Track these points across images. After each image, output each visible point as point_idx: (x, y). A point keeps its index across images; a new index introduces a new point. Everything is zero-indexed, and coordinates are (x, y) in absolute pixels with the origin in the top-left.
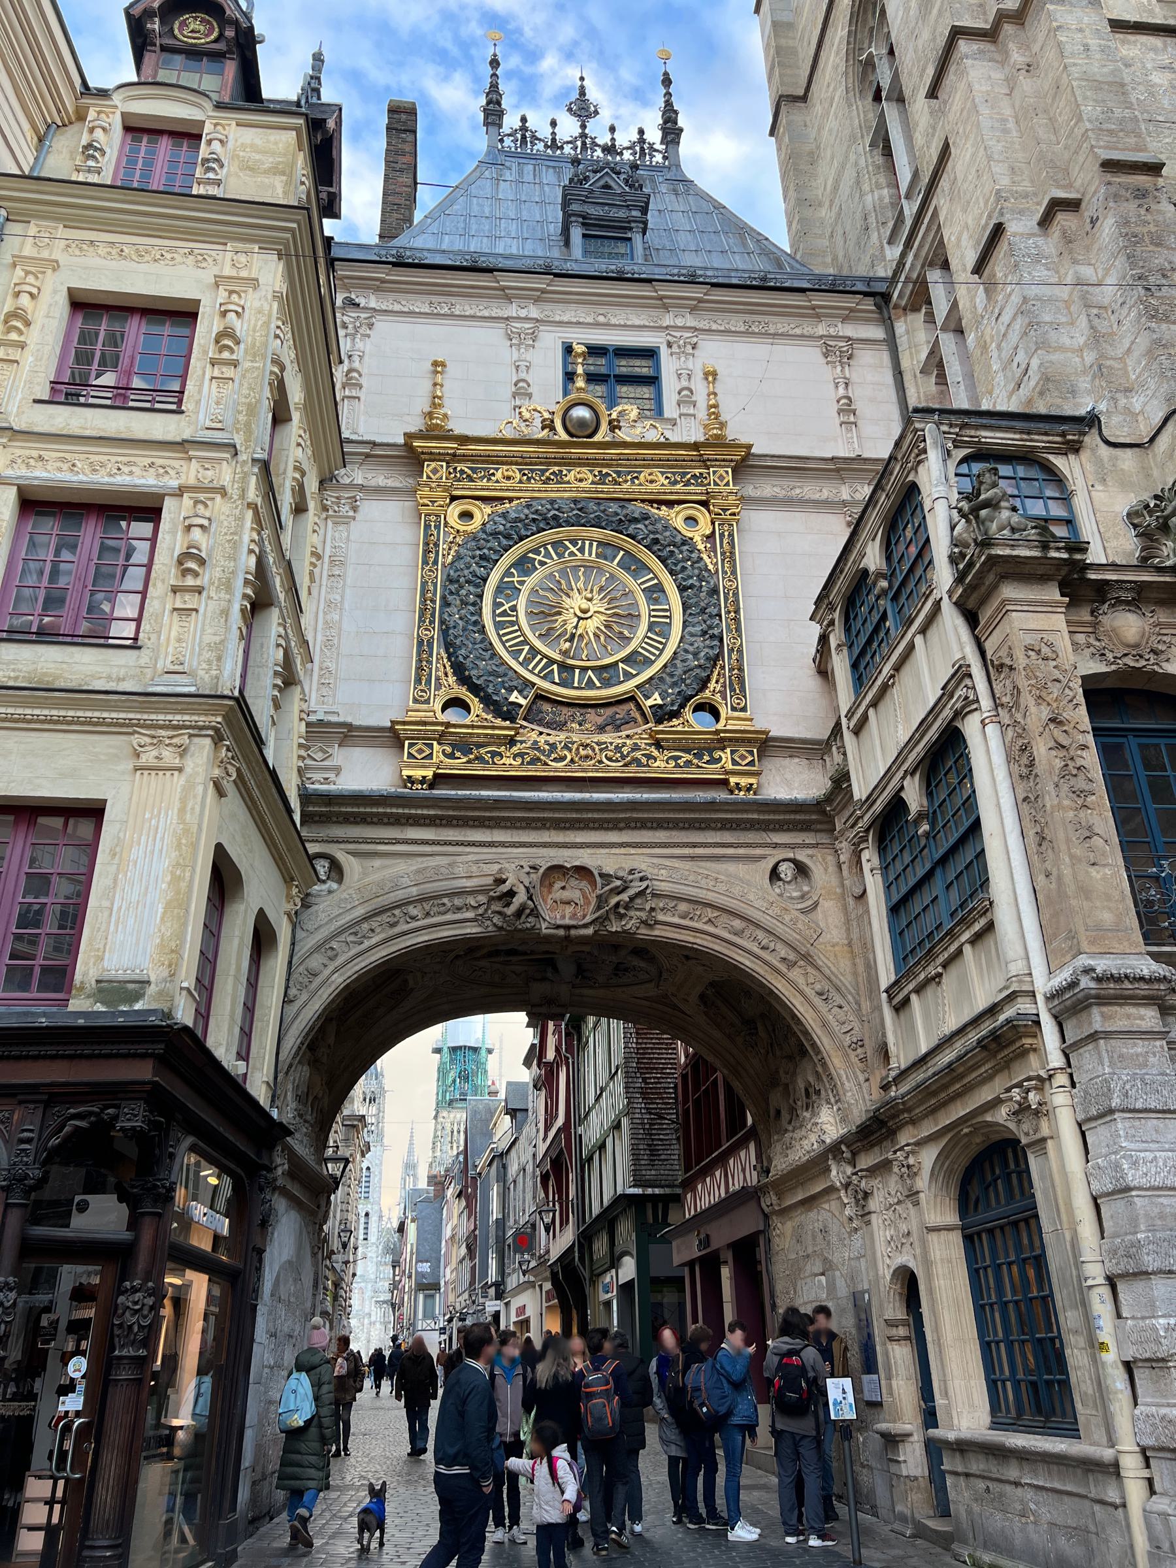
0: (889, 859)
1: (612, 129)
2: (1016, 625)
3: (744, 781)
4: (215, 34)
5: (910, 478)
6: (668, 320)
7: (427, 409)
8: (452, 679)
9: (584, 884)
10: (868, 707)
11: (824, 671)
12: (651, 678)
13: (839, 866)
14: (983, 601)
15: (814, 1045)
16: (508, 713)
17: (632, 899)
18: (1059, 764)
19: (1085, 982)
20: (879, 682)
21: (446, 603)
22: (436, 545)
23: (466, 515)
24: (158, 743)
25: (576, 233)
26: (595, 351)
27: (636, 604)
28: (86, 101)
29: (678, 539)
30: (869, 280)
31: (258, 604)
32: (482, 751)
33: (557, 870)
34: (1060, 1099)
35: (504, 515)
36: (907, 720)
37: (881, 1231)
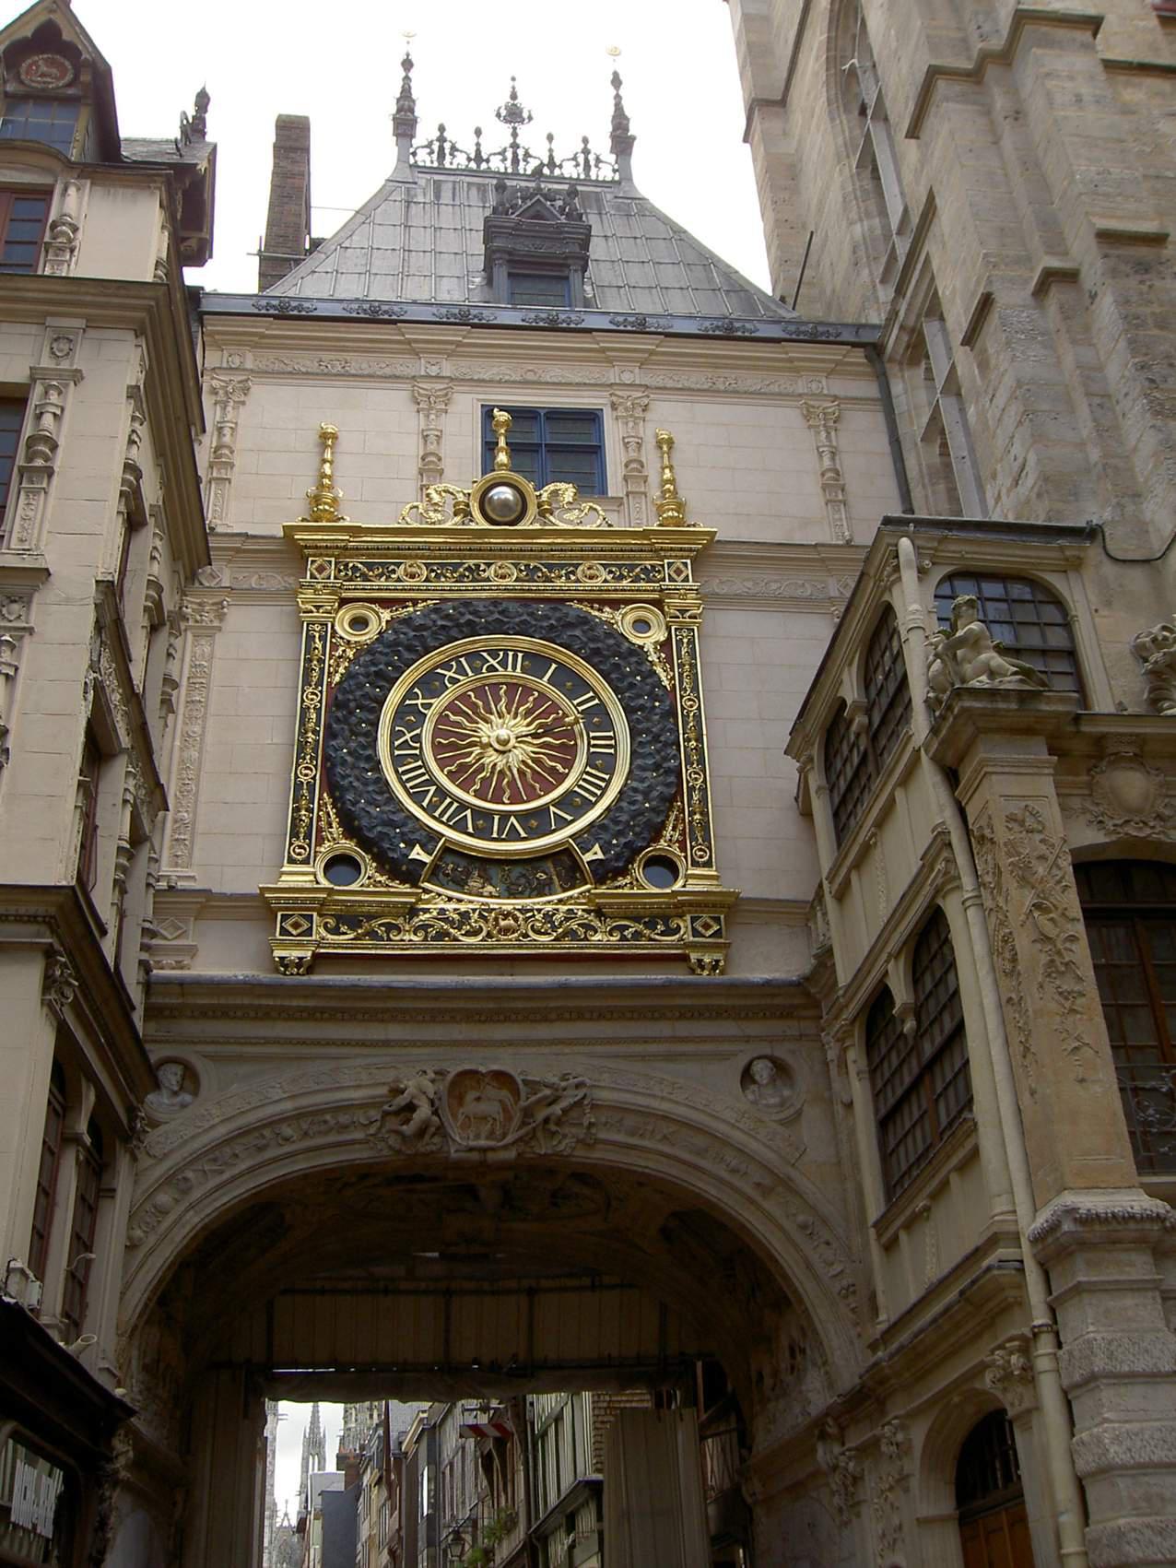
0: (877, 1060)
1: (550, 138)
4: (69, 77)
5: (886, 597)
6: (612, 375)
7: (312, 490)
8: (336, 830)
9: (505, 1094)
10: (849, 872)
11: (807, 814)
12: (592, 824)
14: (961, 759)
15: (796, 1291)
16: (410, 873)
17: (565, 1111)
18: (1044, 959)
19: (1067, 1226)
20: (860, 839)
21: (330, 734)
22: (321, 661)
23: (359, 623)
26: (519, 414)
30: (859, 327)
31: (97, 751)
32: (374, 923)
35: (407, 621)
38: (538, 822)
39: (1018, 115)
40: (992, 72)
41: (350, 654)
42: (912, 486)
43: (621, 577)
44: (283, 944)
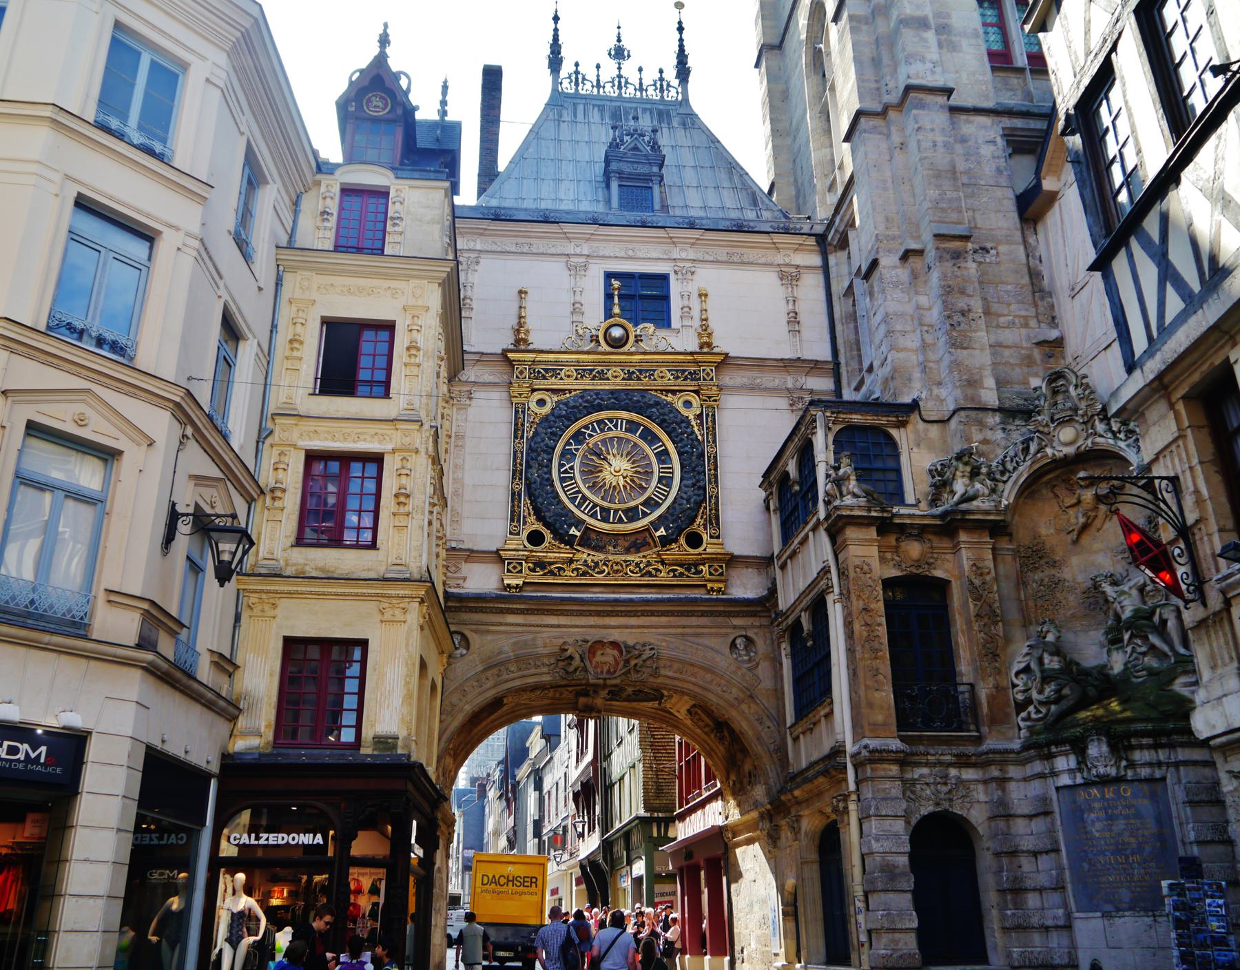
1: (640, 70)
2: (851, 553)
3: (716, 586)
8: (533, 518)
9: (615, 652)
11: (768, 508)
18: (865, 634)
19: (864, 753)
21: (528, 466)
22: (523, 425)
24: (393, 606)
25: (614, 185)
27: (650, 464)
28: (319, 177)
29: (678, 420)
33: (600, 643)
34: (852, 807)
35: (566, 404)
36: (805, 577)
38: (632, 514)
39: (903, 146)
40: (892, 114)
41: (537, 420)
42: (837, 322)
43: (677, 378)
44: (508, 577)
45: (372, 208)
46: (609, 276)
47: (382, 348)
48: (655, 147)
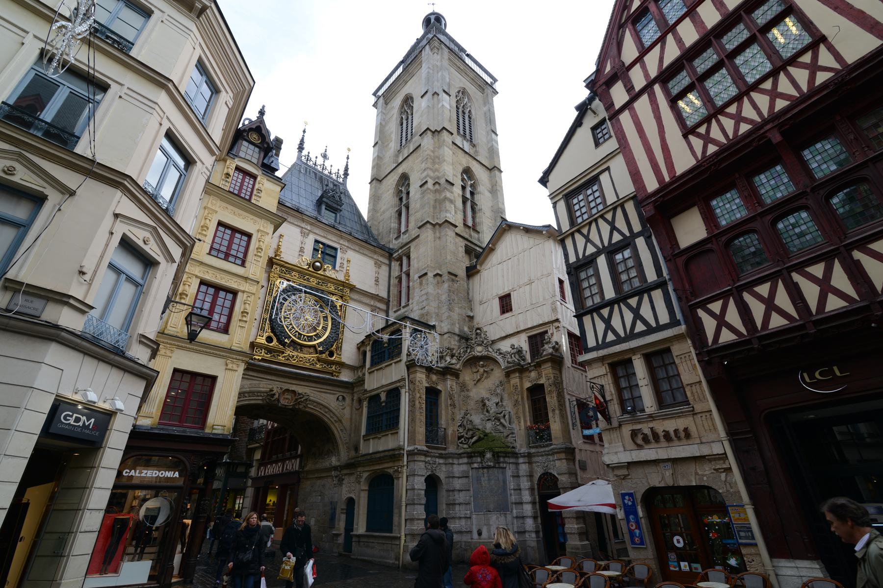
13: (353, 399)
16: (284, 344)
24: (233, 363)
25: (323, 207)
33: (287, 390)
34: (405, 469)
37: (345, 488)
38: (310, 339)
40: (437, 226)
45: (247, 180)
46: (317, 241)
47: (244, 244)
48: (340, 198)
